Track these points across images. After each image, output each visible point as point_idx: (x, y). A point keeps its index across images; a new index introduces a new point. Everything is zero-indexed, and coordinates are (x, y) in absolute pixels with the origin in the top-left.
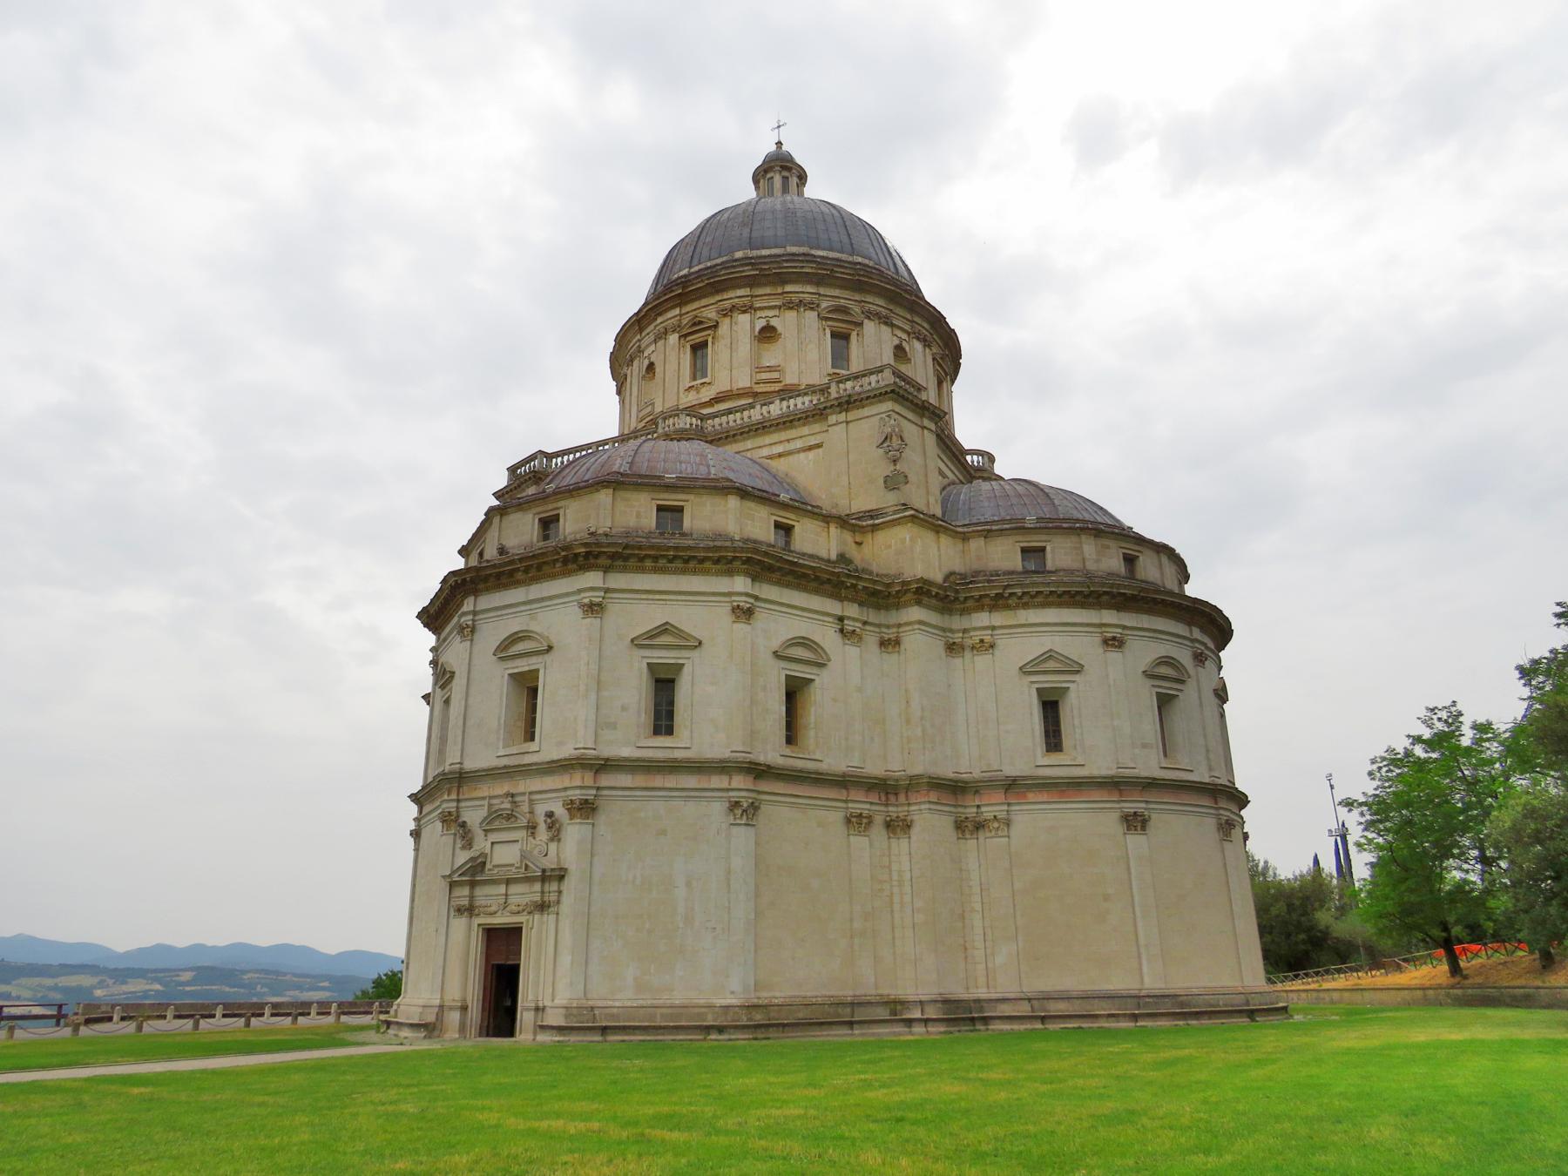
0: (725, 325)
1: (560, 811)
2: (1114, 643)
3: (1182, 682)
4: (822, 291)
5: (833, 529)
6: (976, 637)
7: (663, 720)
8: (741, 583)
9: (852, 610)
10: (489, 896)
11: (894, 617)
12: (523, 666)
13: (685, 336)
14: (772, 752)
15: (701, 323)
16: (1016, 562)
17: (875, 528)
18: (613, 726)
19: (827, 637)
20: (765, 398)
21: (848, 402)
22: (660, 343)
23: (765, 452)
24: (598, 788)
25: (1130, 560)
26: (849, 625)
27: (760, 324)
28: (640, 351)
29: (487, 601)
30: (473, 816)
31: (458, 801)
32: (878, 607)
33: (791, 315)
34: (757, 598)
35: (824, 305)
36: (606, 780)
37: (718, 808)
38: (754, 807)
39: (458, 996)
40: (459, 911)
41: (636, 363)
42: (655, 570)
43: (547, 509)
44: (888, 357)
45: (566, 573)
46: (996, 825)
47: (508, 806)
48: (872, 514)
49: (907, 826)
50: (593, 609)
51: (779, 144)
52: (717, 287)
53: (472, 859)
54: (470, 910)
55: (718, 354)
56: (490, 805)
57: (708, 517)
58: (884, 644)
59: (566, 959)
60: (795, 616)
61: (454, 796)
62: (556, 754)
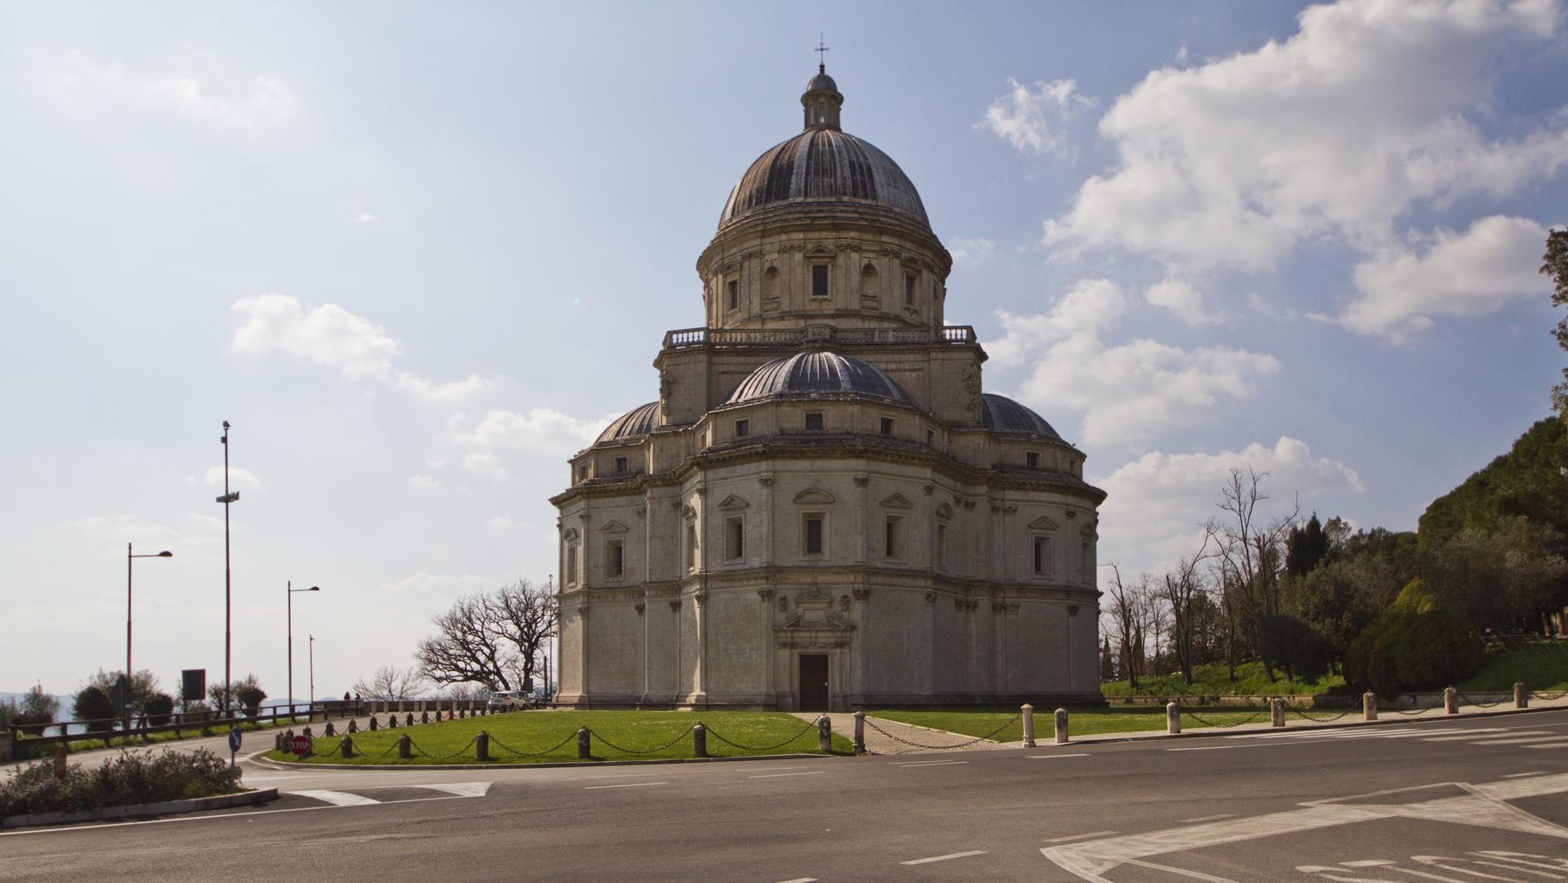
0: (841, 260)
1: (851, 595)
2: (1071, 515)
6: (1008, 504)
8: (928, 472)
10: (801, 636)
11: (971, 490)
12: (813, 509)
16: (1024, 461)
19: (951, 501)
23: (883, 366)
25: (1072, 462)
28: (760, 254)
30: (791, 594)
32: (966, 484)
33: (885, 260)
35: (905, 255)
36: (874, 579)
37: (921, 597)
39: (787, 689)
40: (784, 645)
41: (755, 262)
42: (894, 462)
43: (815, 407)
49: (975, 606)
50: (863, 482)
52: (836, 227)
54: (792, 645)
55: (836, 279)
58: (967, 505)
59: (859, 672)
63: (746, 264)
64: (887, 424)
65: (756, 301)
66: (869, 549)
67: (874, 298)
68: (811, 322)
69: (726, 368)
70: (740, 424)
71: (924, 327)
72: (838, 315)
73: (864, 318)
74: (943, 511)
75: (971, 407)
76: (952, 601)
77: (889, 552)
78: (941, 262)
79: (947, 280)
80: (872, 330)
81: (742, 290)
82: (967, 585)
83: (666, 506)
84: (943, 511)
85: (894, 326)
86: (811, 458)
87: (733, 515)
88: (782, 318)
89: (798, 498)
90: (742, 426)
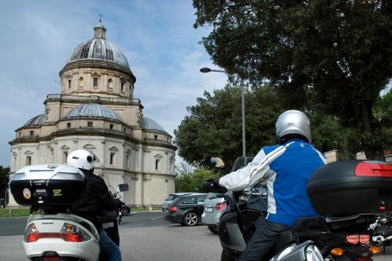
2: (167, 153)
8: (123, 141)
9: (133, 144)
11: (137, 145)
16: (153, 138)
17: (135, 129)
18: (106, 162)
19: (131, 149)
23: (113, 108)
25: (168, 138)
27: (109, 78)
28: (78, 73)
29: (79, 137)
36: (105, 171)
37: (120, 176)
41: (76, 75)
42: (113, 137)
43: (90, 121)
48: (135, 127)
50: (104, 143)
55: (100, 82)
57: (118, 128)
58: (136, 150)
63: (74, 76)
64: (111, 126)
66: (105, 162)
67: (111, 88)
68: (92, 94)
69: (65, 106)
70: (68, 124)
71: (126, 98)
72: (100, 93)
73: (108, 94)
75: (138, 122)
76: (130, 178)
77: (111, 163)
78: (133, 79)
79: (135, 84)
80: (110, 98)
81: (72, 82)
82: (135, 173)
83: (45, 147)
84: (128, 152)
85: (117, 97)
86: (89, 135)
87: (65, 150)
88: (84, 92)
90: (69, 124)
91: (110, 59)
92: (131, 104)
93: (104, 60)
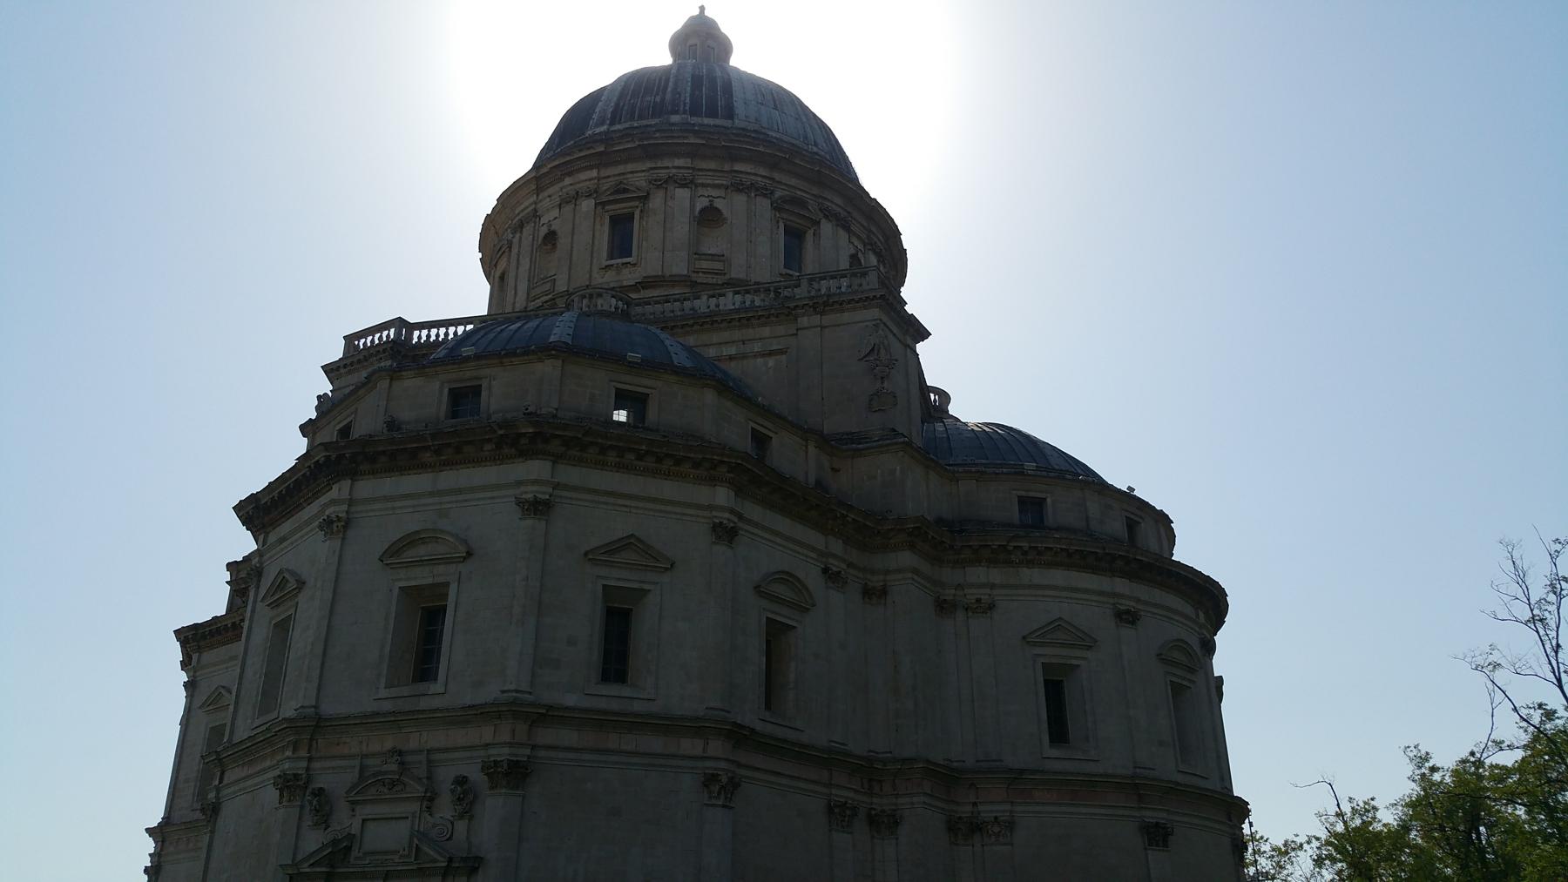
0: (657, 201)
1: (476, 775)
2: (1128, 617)
3: (1192, 670)
4: (777, 176)
5: (811, 449)
7: (615, 661)
8: (722, 496)
9: (837, 546)
13: (603, 204)
14: (750, 715)
15: (625, 191)
16: (1014, 514)
19: (811, 575)
20: (717, 290)
21: (826, 304)
22: (568, 208)
24: (534, 747)
25: (1131, 526)
26: (836, 566)
27: (702, 203)
28: (535, 215)
31: (310, 759)
34: (740, 517)
35: (778, 194)
36: (546, 736)
38: (734, 784)
41: (528, 230)
42: (621, 467)
44: (844, 264)
45: (498, 459)
46: (996, 829)
47: (394, 767)
50: (537, 508)
51: (702, 9)
53: (335, 842)
56: (362, 768)
58: (868, 593)
60: (779, 546)
61: (303, 753)
62: (469, 698)
65: (523, 287)
74: (782, 590)
82: (869, 770)
84: (782, 590)
89: (394, 554)
91: (712, 113)
92: (822, 305)
93: (675, 118)
